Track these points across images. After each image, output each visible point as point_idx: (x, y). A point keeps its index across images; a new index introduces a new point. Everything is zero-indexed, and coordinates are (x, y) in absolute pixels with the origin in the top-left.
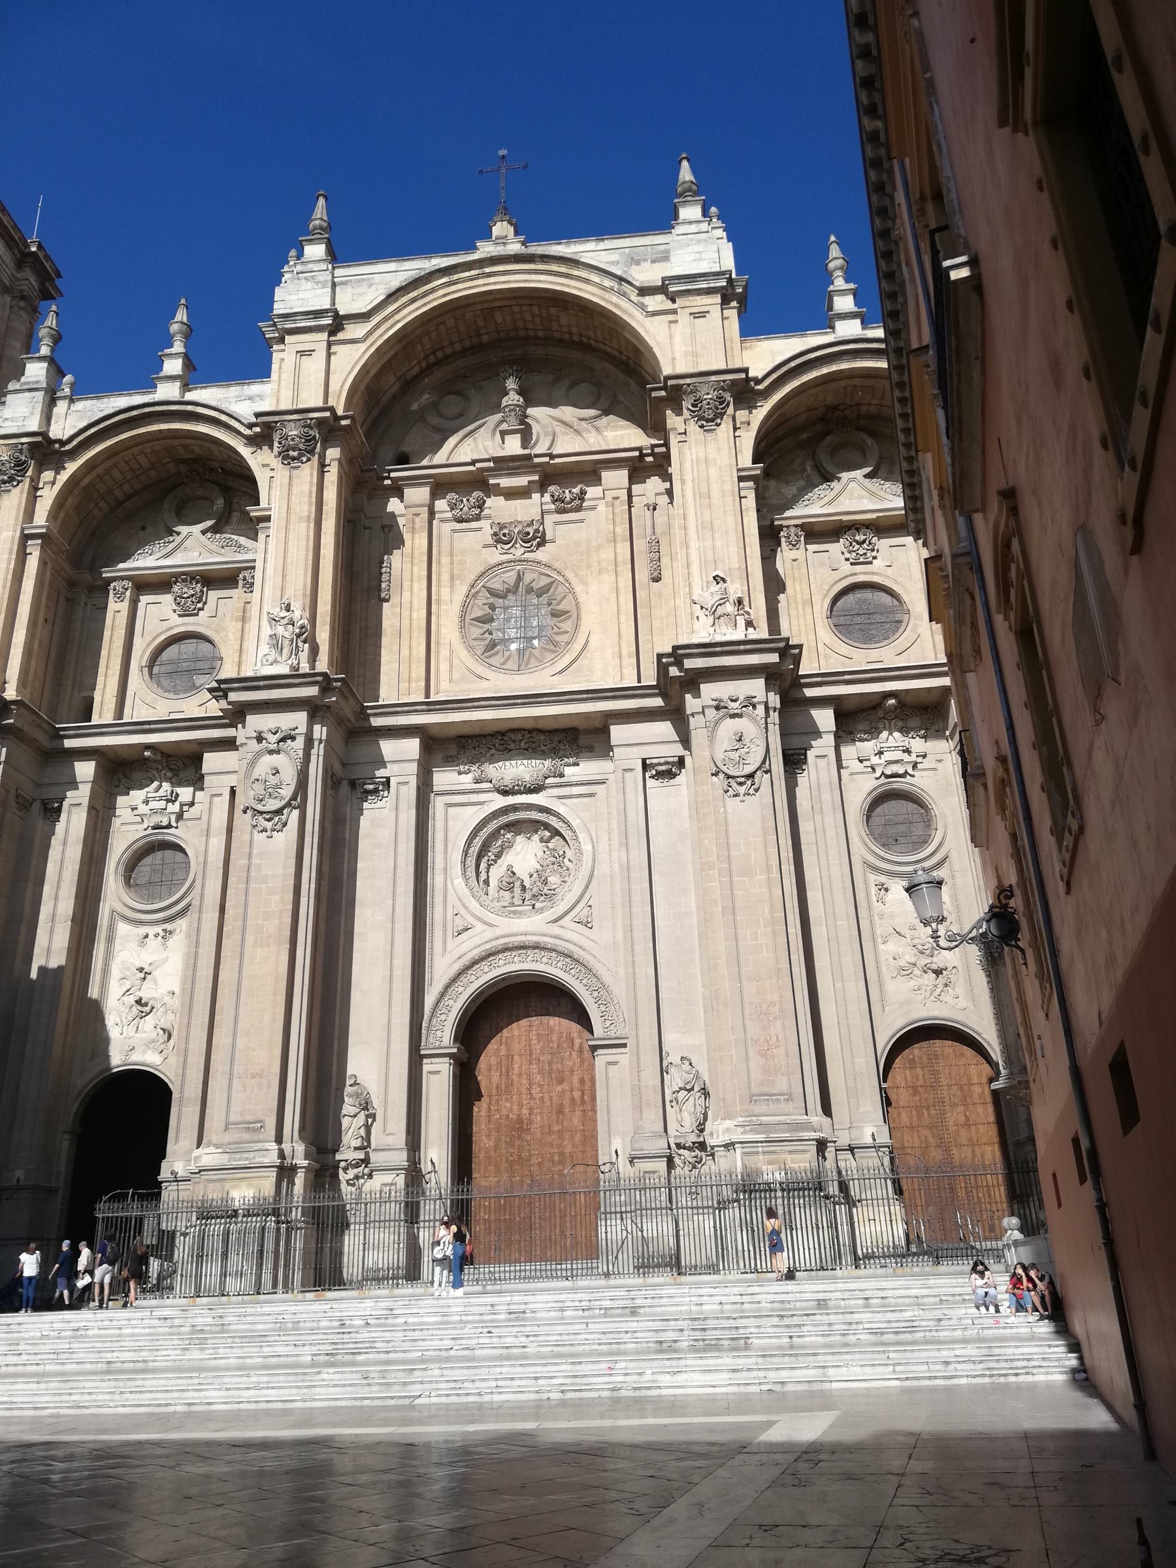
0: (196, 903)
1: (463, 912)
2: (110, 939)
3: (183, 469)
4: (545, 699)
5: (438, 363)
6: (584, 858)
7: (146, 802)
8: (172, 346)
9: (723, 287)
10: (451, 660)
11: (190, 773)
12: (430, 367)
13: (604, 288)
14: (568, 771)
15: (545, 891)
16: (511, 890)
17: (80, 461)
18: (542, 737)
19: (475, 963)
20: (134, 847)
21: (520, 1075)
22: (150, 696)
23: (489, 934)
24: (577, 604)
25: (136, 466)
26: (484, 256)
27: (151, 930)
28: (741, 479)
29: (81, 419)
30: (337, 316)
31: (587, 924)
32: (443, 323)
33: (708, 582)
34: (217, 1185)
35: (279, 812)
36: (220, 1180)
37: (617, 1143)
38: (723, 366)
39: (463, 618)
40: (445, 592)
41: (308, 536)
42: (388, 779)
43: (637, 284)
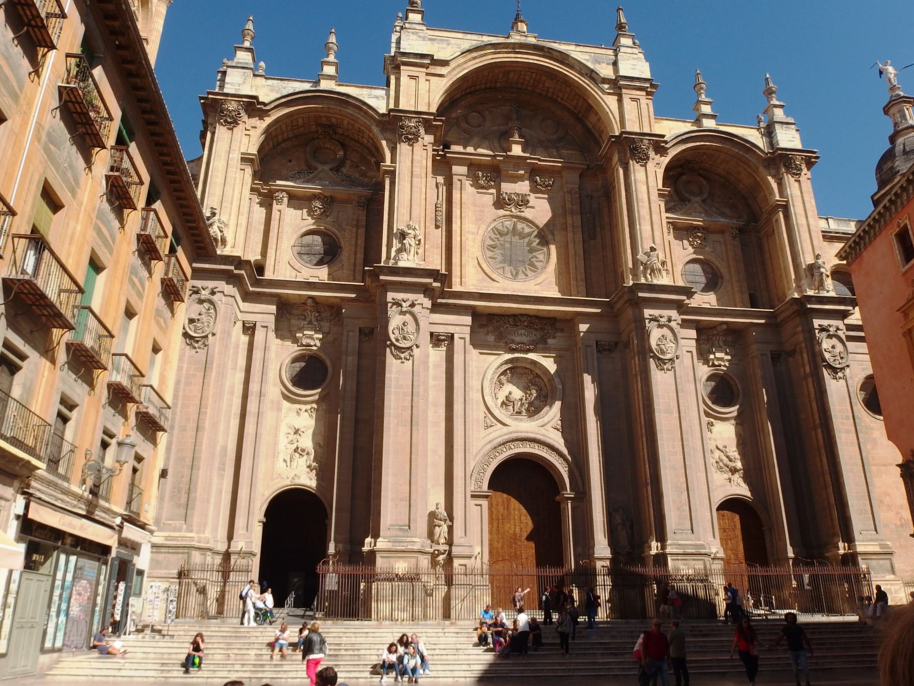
2: (279, 409)
3: (320, 129)
5: (470, 93)
8: (328, 56)
9: (648, 87)
12: (466, 94)
14: (550, 341)
18: (537, 321)
21: (514, 509)
22: (298, 265)
26: (517, 41)
27: (304, 407)
29: (272, 90)
34: (385, 560)
35: (410, 348)
42: (453, 335)
43: (602, 75)
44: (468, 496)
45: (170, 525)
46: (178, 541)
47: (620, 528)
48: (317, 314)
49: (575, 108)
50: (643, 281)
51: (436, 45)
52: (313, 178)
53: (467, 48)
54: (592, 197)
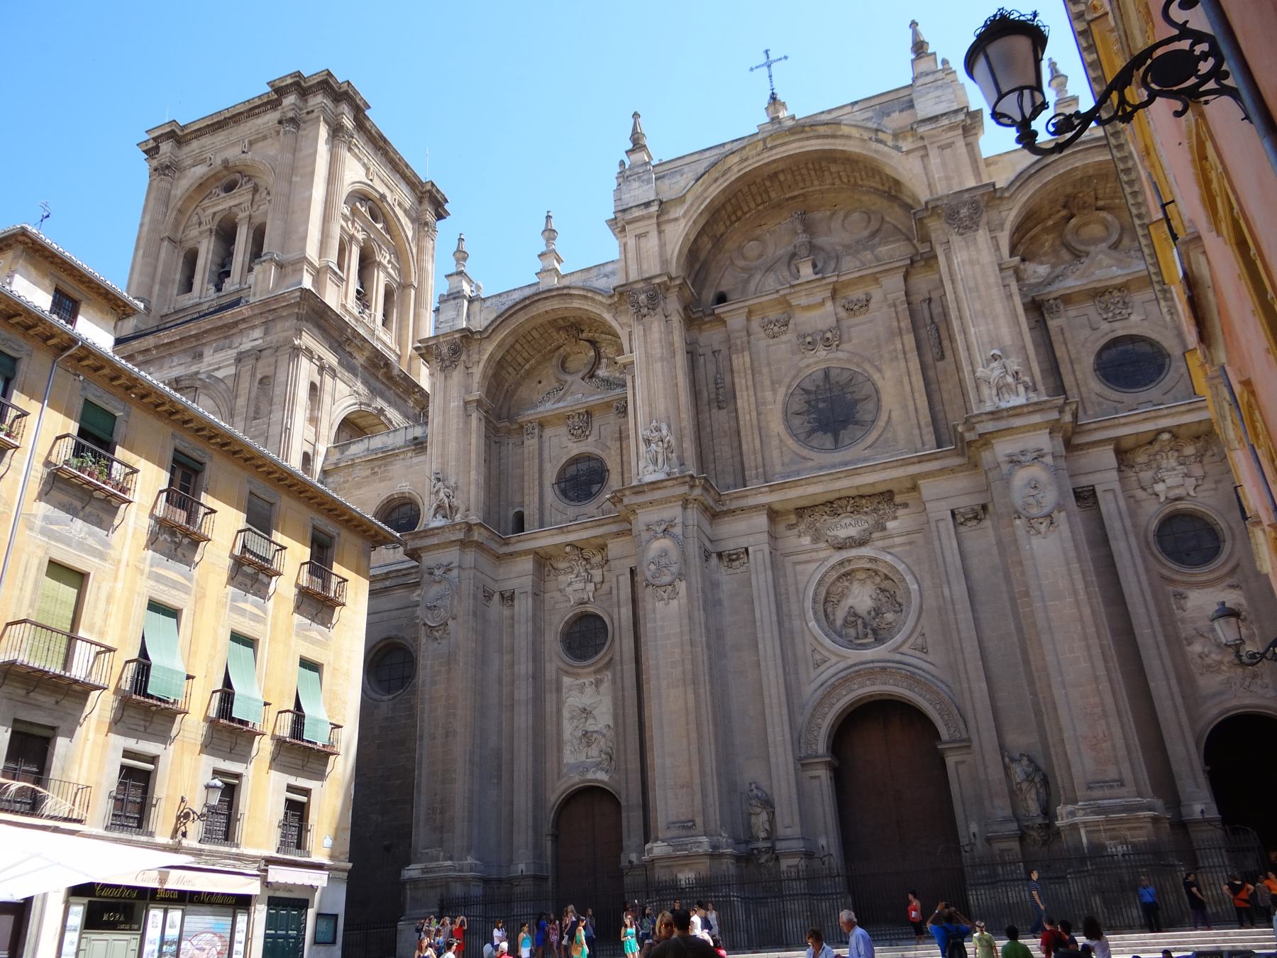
0: (617, 658)
1: (819, 648)
2: (559, 690)
3: (563, 334)
4: (863, 470)
6: (913, 596)
7: (570, 584)
10: (781, 448)
11: (597, 559)
13: (863, 140)
14: (890, 525)
15: (883, 626)
16: (855, 624)
17: (495, 344)
18: (864, 501)
19: (834, 687)
20: (566, 619)
22: (561, 506)
23: (842, 665)
24: (877, 392)
25: (530, 338)
28: (1001, 270)
30: (661, 203)
31: (923, 649)
32: (741, 191)
33: (987, 360)
36: (668, 866)
37: (974, 828)
38: (971, 183)
39: (786, 413)
40: (769, 395)
41: (663, 373)
42: (747, 550)
44: (791, 766)
45: (427, 854)
46: (435, 872)
47: (1025, 786)
48: (584, 563)
49: (883, 185)
50: (989, 407)
51: (667, 181)
52: (564, 395)
53: (703, 171)
54: (930, 300)
